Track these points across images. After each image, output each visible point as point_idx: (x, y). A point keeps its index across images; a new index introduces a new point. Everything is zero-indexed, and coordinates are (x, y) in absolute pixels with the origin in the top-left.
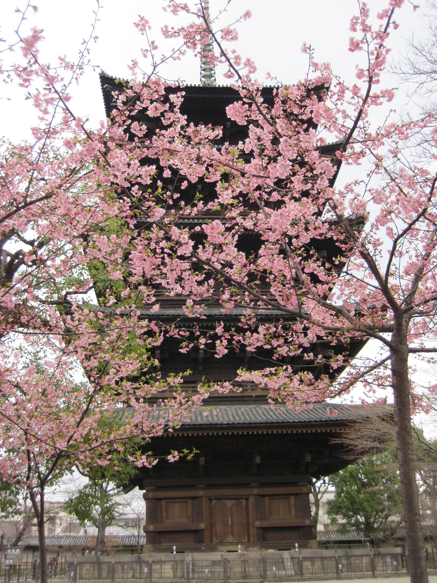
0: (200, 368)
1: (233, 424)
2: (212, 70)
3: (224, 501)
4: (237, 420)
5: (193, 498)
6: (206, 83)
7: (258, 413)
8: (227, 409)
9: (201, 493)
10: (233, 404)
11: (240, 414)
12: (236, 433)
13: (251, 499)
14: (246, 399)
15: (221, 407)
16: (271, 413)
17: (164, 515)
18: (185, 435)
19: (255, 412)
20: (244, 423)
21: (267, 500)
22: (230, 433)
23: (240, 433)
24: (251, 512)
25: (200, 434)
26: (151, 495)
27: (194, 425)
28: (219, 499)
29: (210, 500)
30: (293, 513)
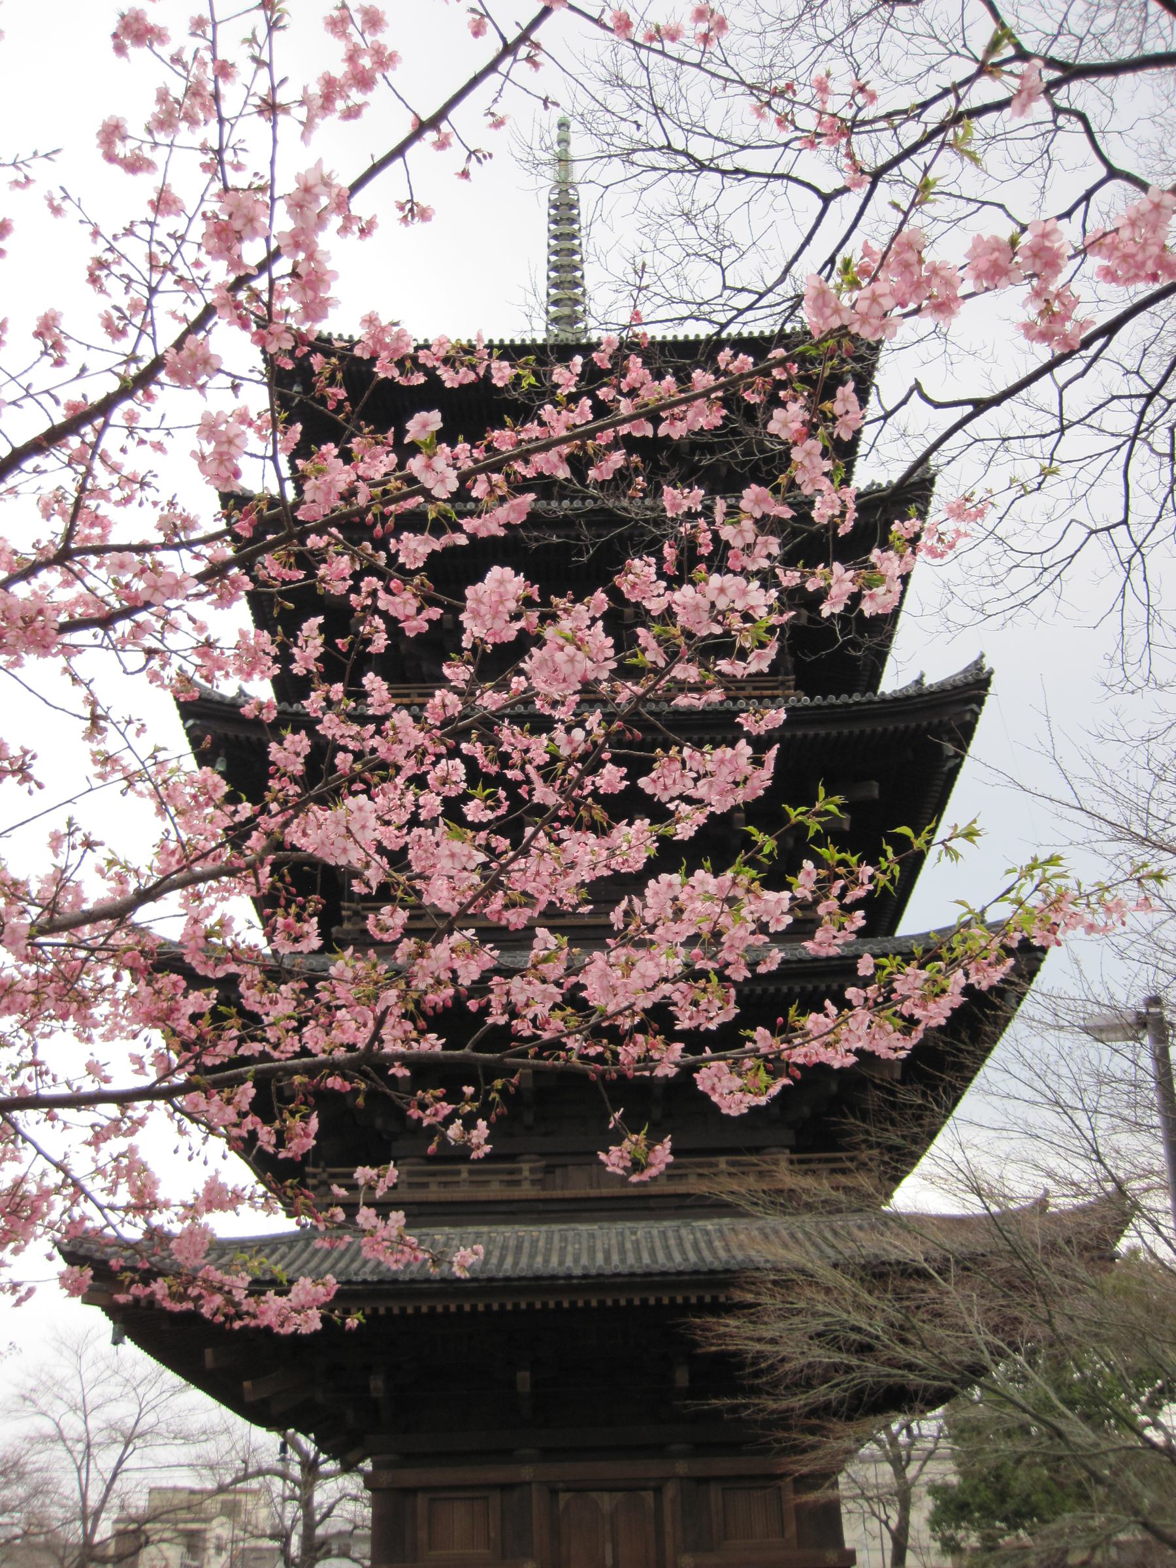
0: (529, 1118)
1: (599, 1275)
2: (577, 302)
3: (593, 1495)
4: (616, 1264)
5: (505, 1488)
6: (562, 336)
7: (680, 1244)
8: (598, 1233)
9: (527, 1472)
10: (614, 1220)
11: (628, 1245)
12: (609, 1303)
13: (670, 1491)
14: (652, 1203)
15: (582, 1228)
16: (717, 1244)
17: (423, 1535)
18: (467, 1308)
19: (672, 1242)
20: (632, 1275)
21: (715, 1493)
22: (594, 1303)
23: (623, 1302)
24: (668, 1528)
25: (509, 1307)
26: (385, 1478)
27: (491, 1280)
28: (580, 1488)
29: (554, 1492)
30: (792, 1529)
